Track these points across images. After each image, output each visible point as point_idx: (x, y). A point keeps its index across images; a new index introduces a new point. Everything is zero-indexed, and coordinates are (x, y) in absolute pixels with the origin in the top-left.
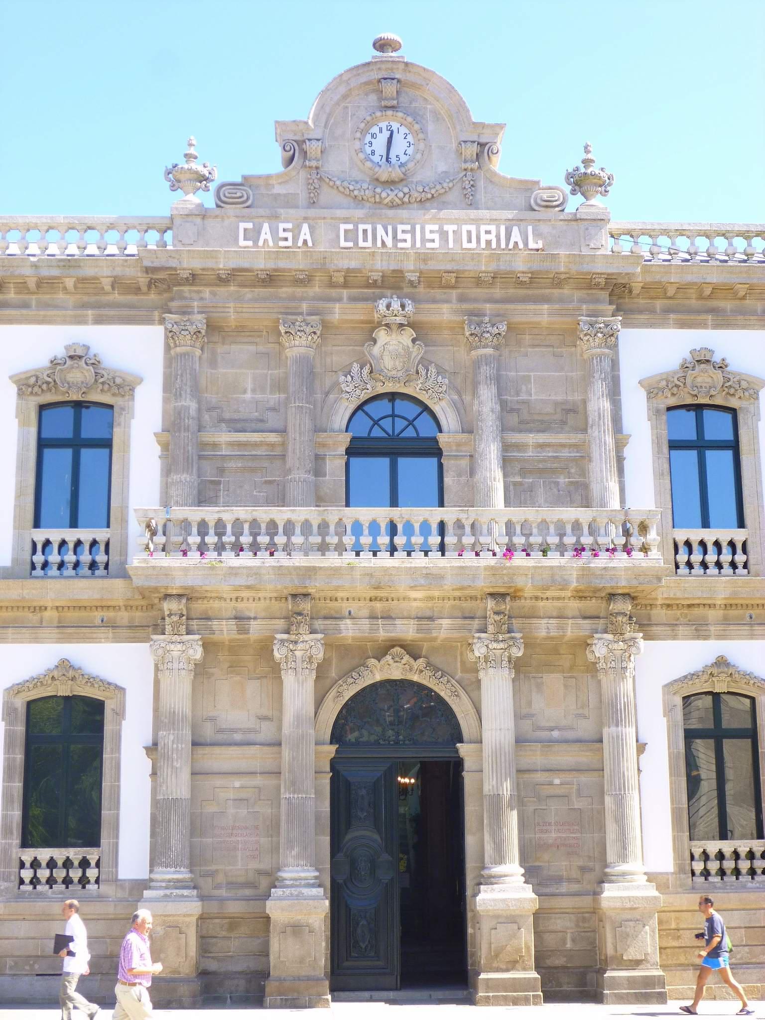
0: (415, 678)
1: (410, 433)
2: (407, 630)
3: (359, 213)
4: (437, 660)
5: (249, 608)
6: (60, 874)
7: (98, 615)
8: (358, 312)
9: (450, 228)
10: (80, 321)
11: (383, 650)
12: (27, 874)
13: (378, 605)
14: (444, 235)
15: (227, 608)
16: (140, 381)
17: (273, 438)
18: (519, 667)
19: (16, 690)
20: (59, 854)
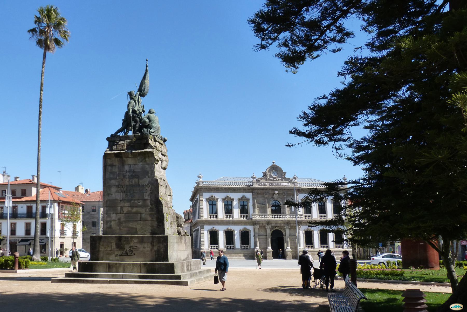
0: (279, 229)
1: (277, 204)
2: (278, 225)
3: (272, 182)
4: (281, 227)
5: (263, 223)
6: (245, 248)
7: (248, 223)
8: (272, 192)
9: (281, 183)
10: (244, 193)
11: (276, 227)
12: (242, 248)
13: (276, 223)
14: (281, 184)
15: (261, 223)
16: (250, 199)
17: (264, 205)
18: (289, 228)
19: (240, 230)
20: (245, 246)
